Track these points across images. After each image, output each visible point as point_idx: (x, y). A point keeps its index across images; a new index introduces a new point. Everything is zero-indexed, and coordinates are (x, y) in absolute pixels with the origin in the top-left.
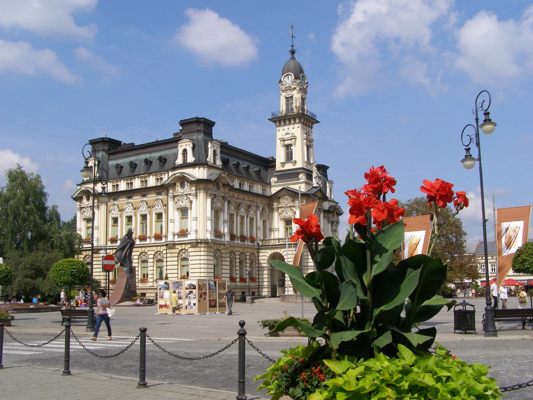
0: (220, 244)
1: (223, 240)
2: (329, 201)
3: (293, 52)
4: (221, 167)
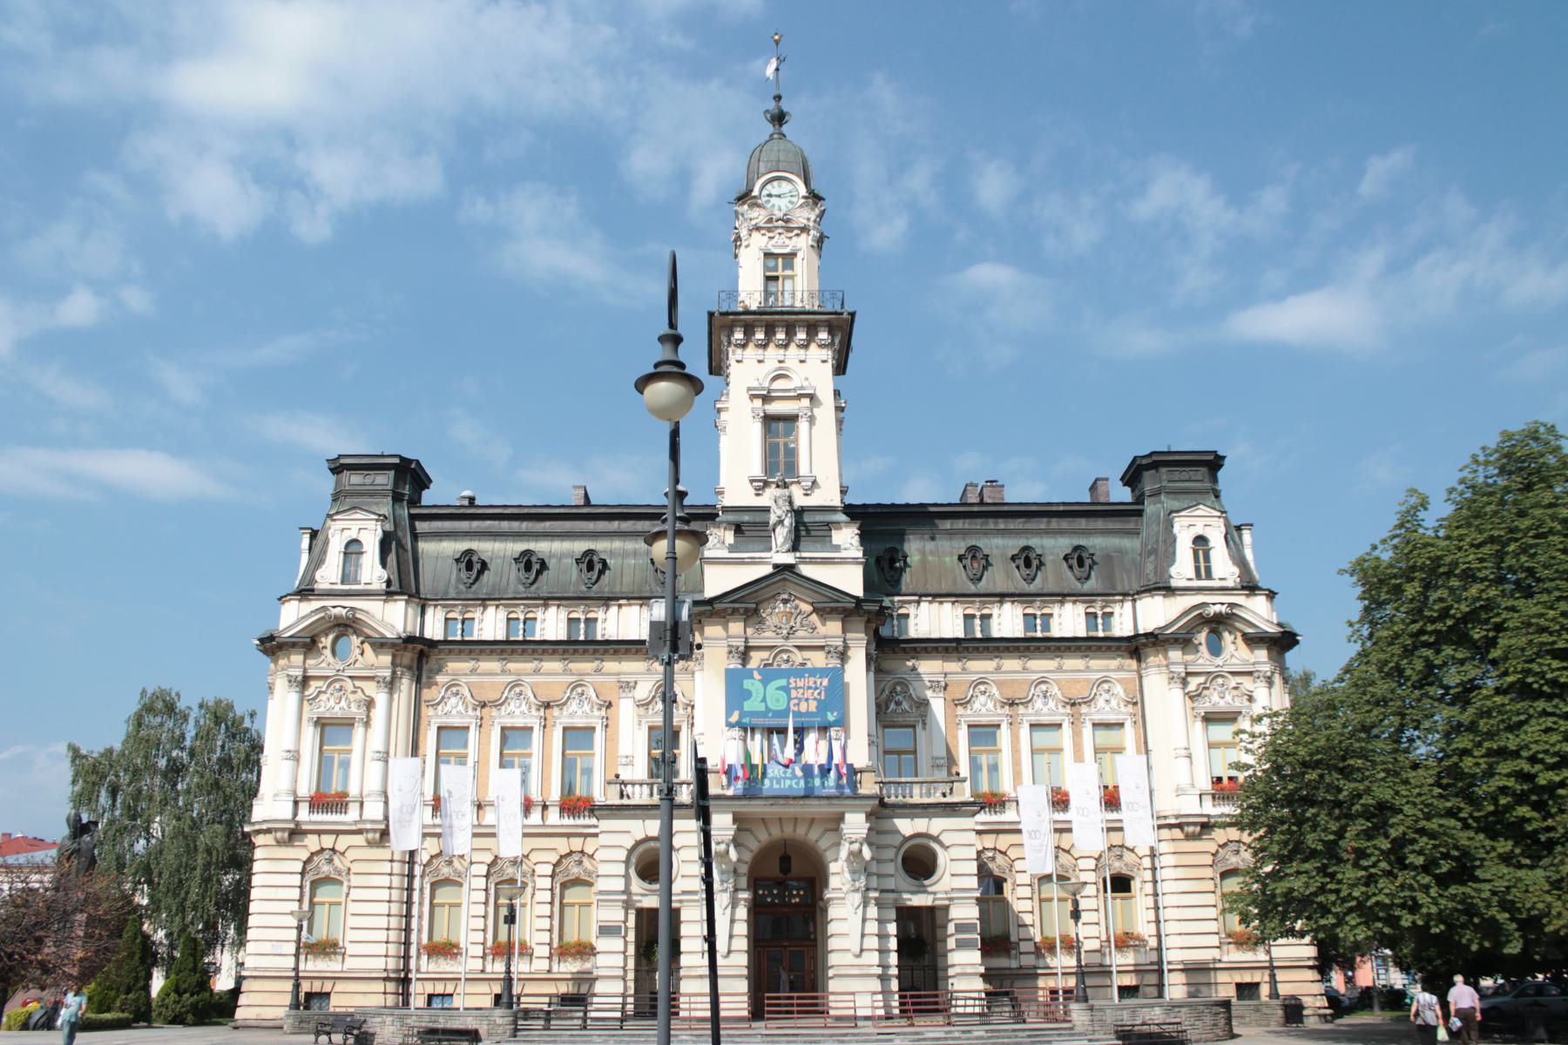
0: (338, 833)
1: (353, 814)
2: (1169, 591)
3: (779, 118)
4: (384, 586)
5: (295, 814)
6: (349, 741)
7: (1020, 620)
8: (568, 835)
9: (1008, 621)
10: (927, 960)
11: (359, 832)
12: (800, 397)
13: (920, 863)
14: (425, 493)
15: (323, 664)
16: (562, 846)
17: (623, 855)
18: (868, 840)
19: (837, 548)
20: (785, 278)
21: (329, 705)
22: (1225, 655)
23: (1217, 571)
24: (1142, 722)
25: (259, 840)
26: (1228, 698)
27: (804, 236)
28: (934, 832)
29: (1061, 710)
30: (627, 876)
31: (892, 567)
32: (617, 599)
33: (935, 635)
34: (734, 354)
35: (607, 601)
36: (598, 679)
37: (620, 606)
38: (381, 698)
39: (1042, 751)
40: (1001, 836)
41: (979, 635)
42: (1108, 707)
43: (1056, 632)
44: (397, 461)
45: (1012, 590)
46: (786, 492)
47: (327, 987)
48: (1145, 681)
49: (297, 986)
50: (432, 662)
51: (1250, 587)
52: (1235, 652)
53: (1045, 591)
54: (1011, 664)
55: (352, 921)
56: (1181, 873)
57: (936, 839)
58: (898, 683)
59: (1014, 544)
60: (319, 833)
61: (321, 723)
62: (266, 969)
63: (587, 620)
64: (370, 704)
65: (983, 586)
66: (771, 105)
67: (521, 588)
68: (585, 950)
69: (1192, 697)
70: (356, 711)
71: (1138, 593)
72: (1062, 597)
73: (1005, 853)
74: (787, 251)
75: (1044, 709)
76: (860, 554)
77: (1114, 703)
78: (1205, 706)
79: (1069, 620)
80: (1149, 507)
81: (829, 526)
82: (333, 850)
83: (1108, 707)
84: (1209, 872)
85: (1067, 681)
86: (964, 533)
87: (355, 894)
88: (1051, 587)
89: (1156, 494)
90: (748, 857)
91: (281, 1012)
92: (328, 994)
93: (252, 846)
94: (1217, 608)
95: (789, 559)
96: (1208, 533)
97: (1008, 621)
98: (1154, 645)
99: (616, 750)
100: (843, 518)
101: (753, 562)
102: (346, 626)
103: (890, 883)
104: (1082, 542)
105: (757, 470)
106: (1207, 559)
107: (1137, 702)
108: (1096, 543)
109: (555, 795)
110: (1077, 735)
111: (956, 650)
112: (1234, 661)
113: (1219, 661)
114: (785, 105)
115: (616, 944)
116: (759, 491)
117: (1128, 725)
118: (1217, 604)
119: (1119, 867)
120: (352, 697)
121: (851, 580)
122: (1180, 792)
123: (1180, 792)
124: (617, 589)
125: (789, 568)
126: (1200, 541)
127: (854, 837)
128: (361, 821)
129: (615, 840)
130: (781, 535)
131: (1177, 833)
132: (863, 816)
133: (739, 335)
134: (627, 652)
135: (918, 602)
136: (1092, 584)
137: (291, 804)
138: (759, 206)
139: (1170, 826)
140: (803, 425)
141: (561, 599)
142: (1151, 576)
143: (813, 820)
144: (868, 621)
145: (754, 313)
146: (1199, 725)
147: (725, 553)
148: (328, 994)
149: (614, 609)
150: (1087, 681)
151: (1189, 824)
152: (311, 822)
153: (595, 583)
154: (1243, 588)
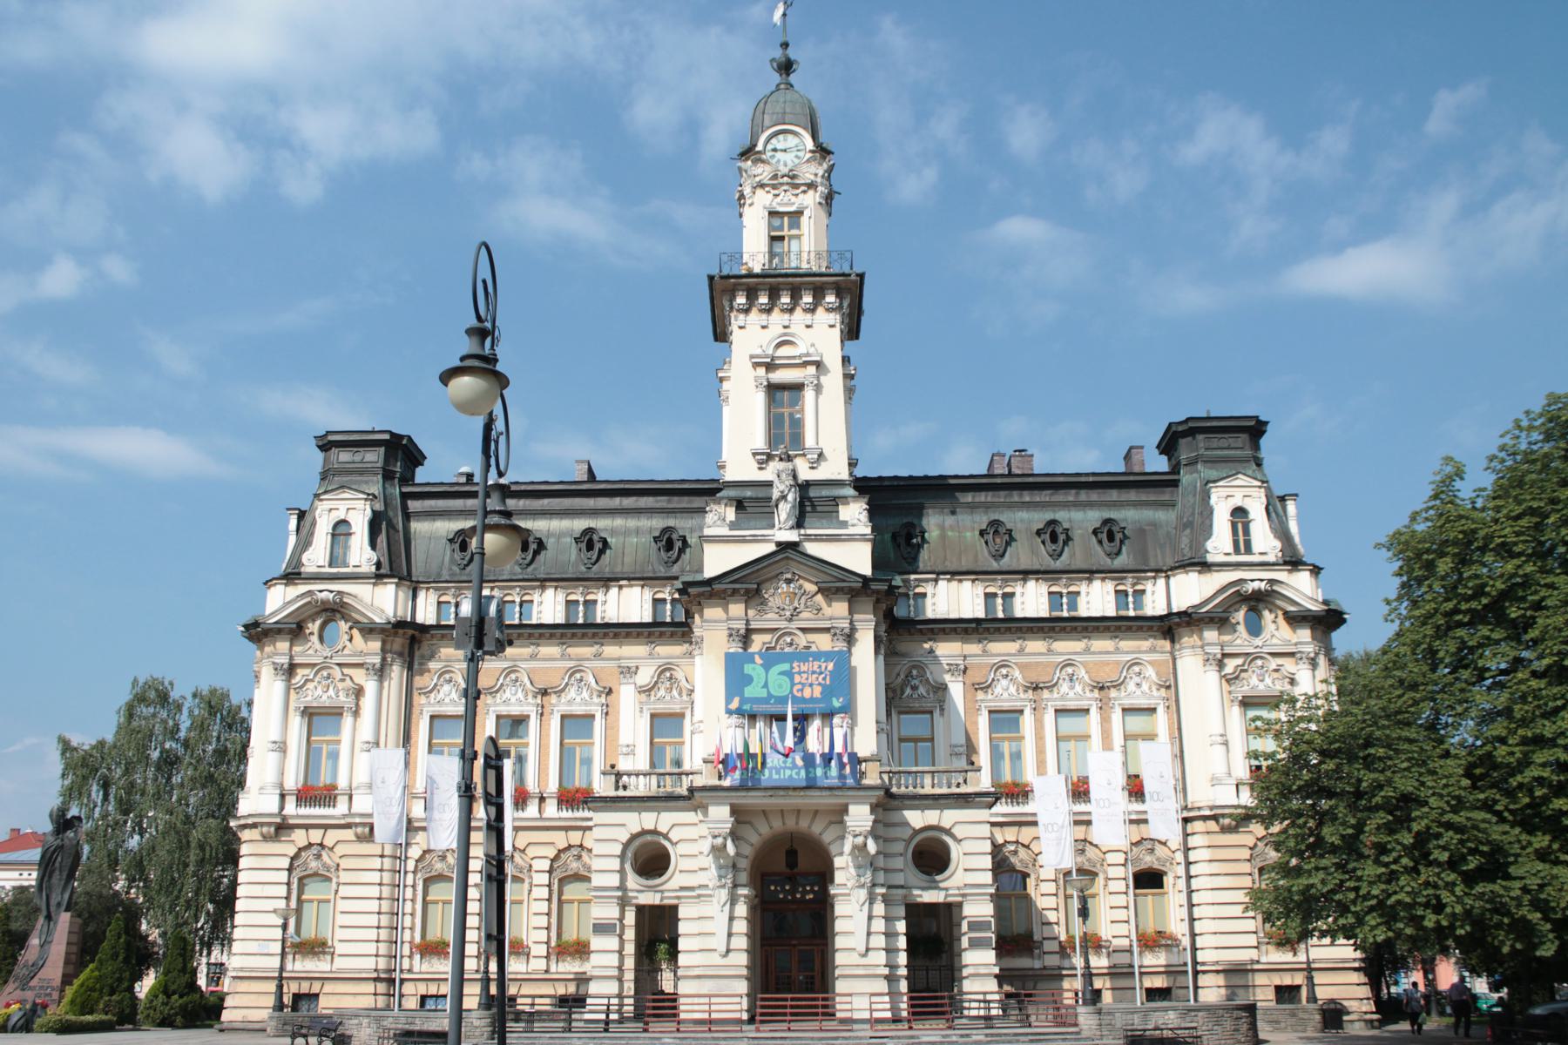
0: (326, 827)
1: (341, 807)
2: (1205, 566)
3: (786, 67)
5: (282, 808)
6: (338, 732)
7: (1045, 600)
8: (567, 829)
9: (1032, 600)
10: (944, 960)
11: (348, 826)
12: (805, 364)
13: (932, 857)
14: (419, 470)
15: (310, 650)
16: (560, 839)
17: (618, 849)
18: (874, 833)
19: (844, 524)
20: (791, 237)
21: (317, 694)
22: (1265, 635)
23: (1257, 546)
24: (1175, 707)
25: (245, 835)
26: (1268, 681)
27: (811, 192)
28: (946, 824)
29: (1088, 694)
30: (622, 871)
31: (908, 543)
32: (617, 580)
33: (953, 616)
34: (736, 320)
35: (606, 581)
36: (597, 664)
37: (620, 587)
38: (370, 686)
39: (1068, 738)
40: (1024, 829)
41: (1001, 615)
42: (1138, 691)
43: (1083, 611)
44: (387, 437)
45: (1036, 567)
46: (789, 465)
47: (316, 988)
48: (1179, 663)
49: (280, 987)
50: (425, 649)
51: (1293, 562)
52: (1277, 632)
53: (1073, 567)
54: (1036, 646)
55: (342, 920)
56: (1216, 868)
57: (948, 832)
58: (914, 667)
59: (1039, 518)
60: (307, 827)
61: (309, 713)
62: (252, 970)
63: (586, 602)
64: (359, 692)
65: (1006, 562)
66: (778, 53)
67: (517, 569)
68: (581, 950)
69: (1230, 680)
70: (345, 700)
71: (1172, 569)
72: (1090, 574)
73: (1027, 847)
74: (792, 209)
75: (1071, 693)
76: (868, 530)
77: (1145, 687)
78: (1243, 689)
79: (1097, 599)
80: (1186, 477)
81: (835, 501)
82: (321, 845)
83: (1138, 691)
84: (1246, 867)
85: (1096, 663)
86: (987, 506)
87: (343, 891)
88: (1079, 563)
89: (1192, 463)
90: (748, 850)
91: (264, 1014)
92: (317, 995)
93: (239, 841)
94: (1256, 585)
95: (792, 536)
96: (1248, 504)
97: (1032, 600)
98: (1188, 624)
99: (617, 739)
100: (850, 491)
101: (755, 540)
102: (334, 611)
103: (899, 879)
104: (1113, 515)
105: (760, 443)
106: (1247, 532)
107: (1170, 685)
108: (1128, 516)
109: (553, 786)
110: (1105, 720)
111: (976, 631)
112: (1275, 641)
113: (1258, 641)
114: (792, 53)
115: (612, 943)
116: (762, 465)
117: (1161, 710)
118: (1256, 580)
119: (1148, 861)
120: (341, 685)
121: (858, 558)
122: (1215, 782)
123: (1215, 782)
124: (619, 569)
125: (793, 546)
126: (1239, 513)
127: (858, 830)
128: (350, 815)
129: (610, 833)
130: (784, 511)
131: (1212, 825)
132: (867, 808)
133: (741, 300)
134: (628, 635)
135: (936, 581)
136: (1123, 560)
137: (277, 798)
138: (763, 161)
139: (1205, 818)
140: (809, 394)
141: (560, 581)
142: (1186, 550)
143: (816, 812)
144: (878, 601)
145: (757, 276)
146: (1236, 709)
147: (725, 531)
148: (317, 995)
149: (614, 591)
150: (1117, 663)
151: (1223, 816)
152: (298, 816)
153: (595, 563)
154: (1285, 563)
